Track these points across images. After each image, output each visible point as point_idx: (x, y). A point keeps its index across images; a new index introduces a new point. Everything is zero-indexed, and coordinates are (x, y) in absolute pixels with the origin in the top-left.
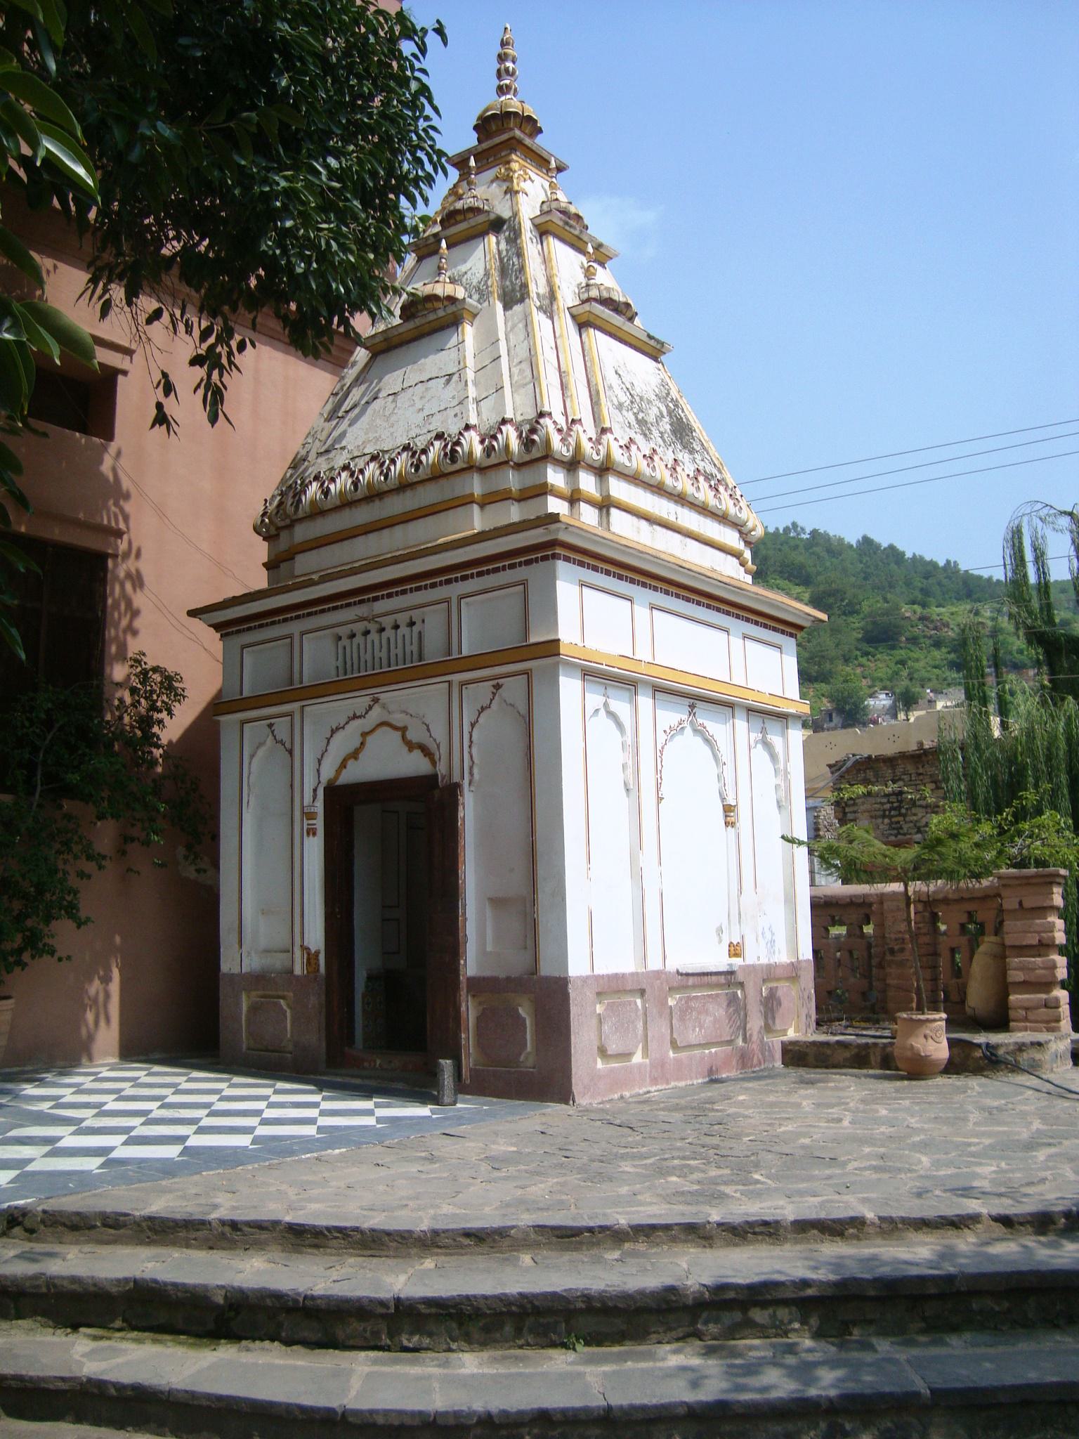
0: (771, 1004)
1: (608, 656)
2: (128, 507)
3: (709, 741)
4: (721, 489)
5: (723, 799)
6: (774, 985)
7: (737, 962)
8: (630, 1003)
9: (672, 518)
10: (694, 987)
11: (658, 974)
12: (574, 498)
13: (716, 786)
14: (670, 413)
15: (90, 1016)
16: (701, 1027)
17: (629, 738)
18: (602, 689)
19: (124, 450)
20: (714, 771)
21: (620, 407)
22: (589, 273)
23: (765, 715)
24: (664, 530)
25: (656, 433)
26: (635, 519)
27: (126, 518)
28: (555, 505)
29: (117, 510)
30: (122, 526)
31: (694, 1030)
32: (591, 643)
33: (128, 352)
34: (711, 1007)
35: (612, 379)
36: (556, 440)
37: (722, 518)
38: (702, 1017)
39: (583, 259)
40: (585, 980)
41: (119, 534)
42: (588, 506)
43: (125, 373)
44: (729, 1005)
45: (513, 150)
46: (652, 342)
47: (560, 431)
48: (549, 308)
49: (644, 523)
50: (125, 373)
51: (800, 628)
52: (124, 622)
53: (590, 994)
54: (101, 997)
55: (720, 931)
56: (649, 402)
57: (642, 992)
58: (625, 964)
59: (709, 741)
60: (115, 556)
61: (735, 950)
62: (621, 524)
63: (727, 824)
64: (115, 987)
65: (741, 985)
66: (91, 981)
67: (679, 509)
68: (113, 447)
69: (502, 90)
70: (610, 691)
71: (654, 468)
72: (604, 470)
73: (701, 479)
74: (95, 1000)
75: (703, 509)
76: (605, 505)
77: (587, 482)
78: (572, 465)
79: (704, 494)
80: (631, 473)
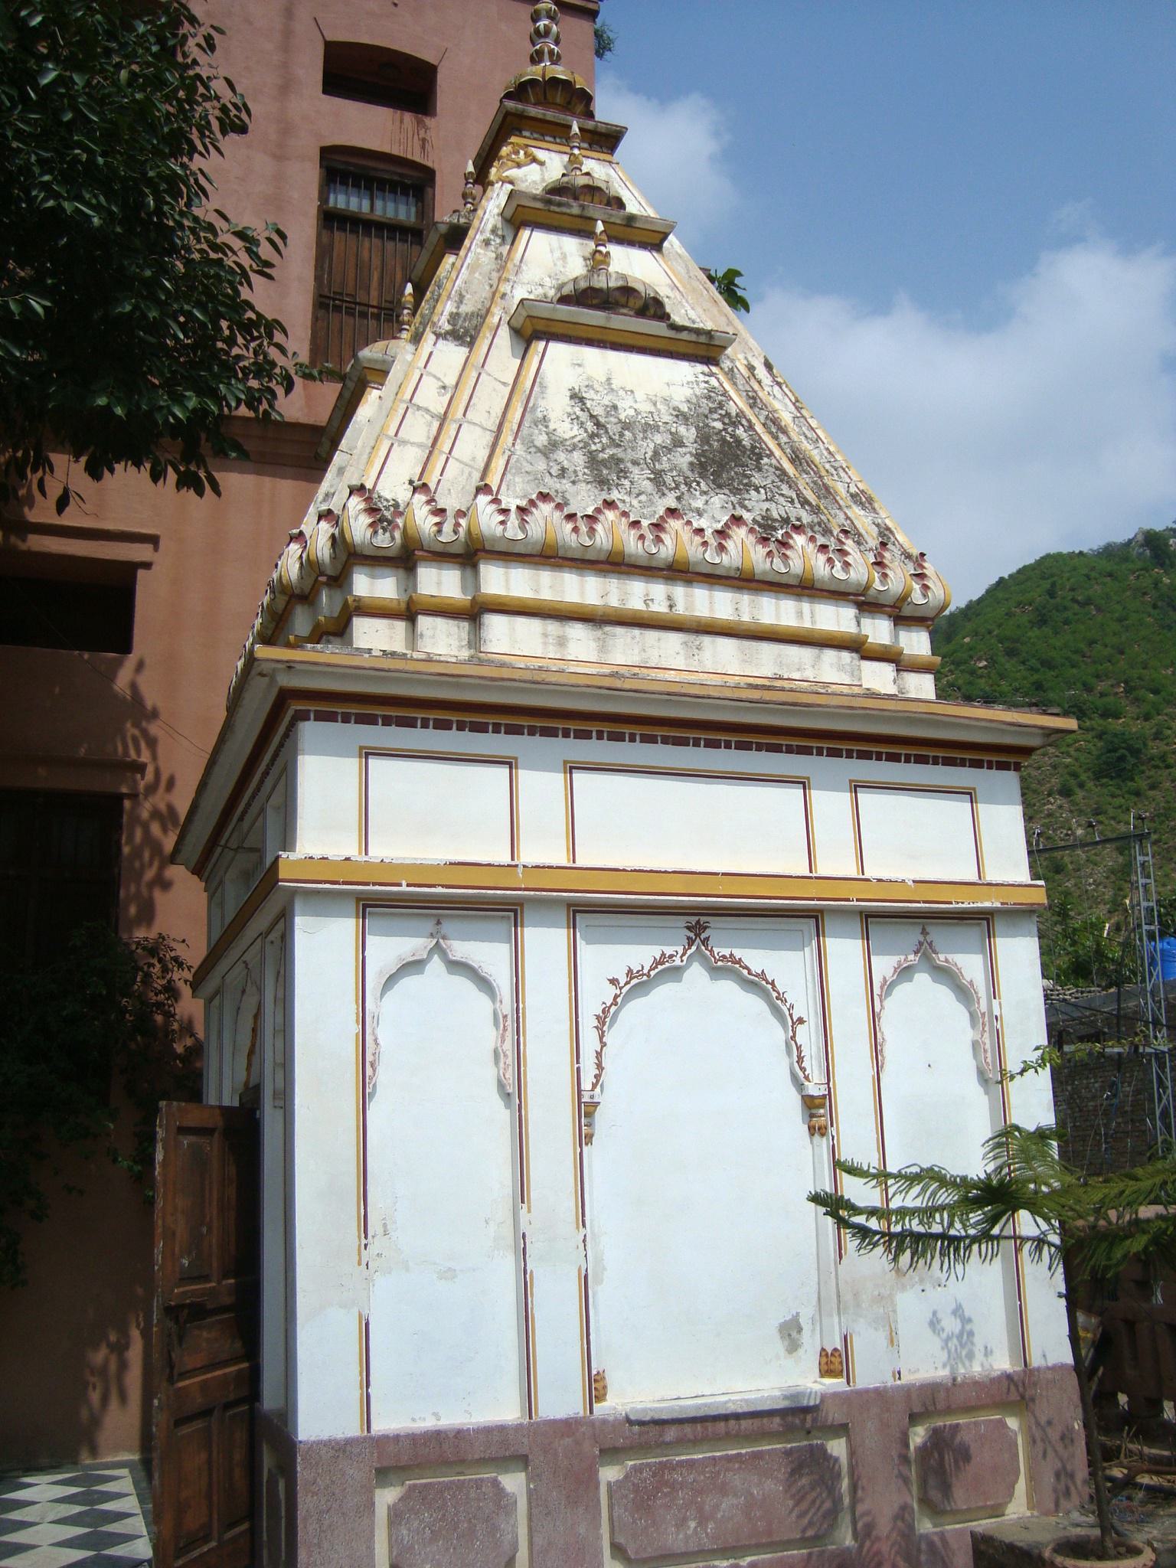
0: (940, 1466)
1: (435, 868)
2: (154, 729)
3: (758, 985)
4: (799, 540)
5: (799, 1086)
6: (940, 1423)
7: (834, 1384)
8: (479, 1484)
9: (660, 607)
10: (681, 1443)
11: (567, 1427)
12: (409, 612)
13: (781, 1067)
14: (704, 438)
15: (95, 1396)
16: (702, 1521)
17: (507, 1007)
18: (429, 925)
19: (147, 662)
20: (779, 1035)
21: (554, 445)
22: (597, 262)
23: (921, 923)
24: (636, 632)
25: (640, 477)
26: (553, 627)
27: (152, 743)
28: (374, 637)
29: (136, 732)
30: (145, 757)
31: (682, 1523)
32: (378, 851)
33: (153, 540)
34: (736, 1480)
35: (556, 406)
36: (359, 527)
37: (805, 588)
38: (709, 1501)
39: (591, 245)
40: (341, 1448)
41: (141, 768)
42: (440, 622)
43: (147, 565)
44: (796, 1472)
45: (518, 131)
46: (684, 335)
47: (372, 510)
48: (465, 333)
49: (577, 632)
50: (147, 565)
51: (1027, 751)
52: (150, 874)
53: (356, 1472)
54: (113, 1367)
55: (790, 1331)
56: (649, 428)
57: (521, 1461)
58: (502, 1409)
59: (758, 985)
60: (134, 796)
61: (834, 1363)
62: (506, 637)
63: (812, 1130)
64: (135, 1354)
65: (841, 1429)
66: (96, 1347)
67: (679, 591)
68: (131, 660)
69: (536, 58)
70: (447, 927)
71: (592, 531)
72: (470, 554)
73: (740, 533)
74: (103, 1371)
75: (744, 581)
76: (473, 613)
77: (440, 582)
78: (406, 558)
79: (744, 550)
80: (537, 549)
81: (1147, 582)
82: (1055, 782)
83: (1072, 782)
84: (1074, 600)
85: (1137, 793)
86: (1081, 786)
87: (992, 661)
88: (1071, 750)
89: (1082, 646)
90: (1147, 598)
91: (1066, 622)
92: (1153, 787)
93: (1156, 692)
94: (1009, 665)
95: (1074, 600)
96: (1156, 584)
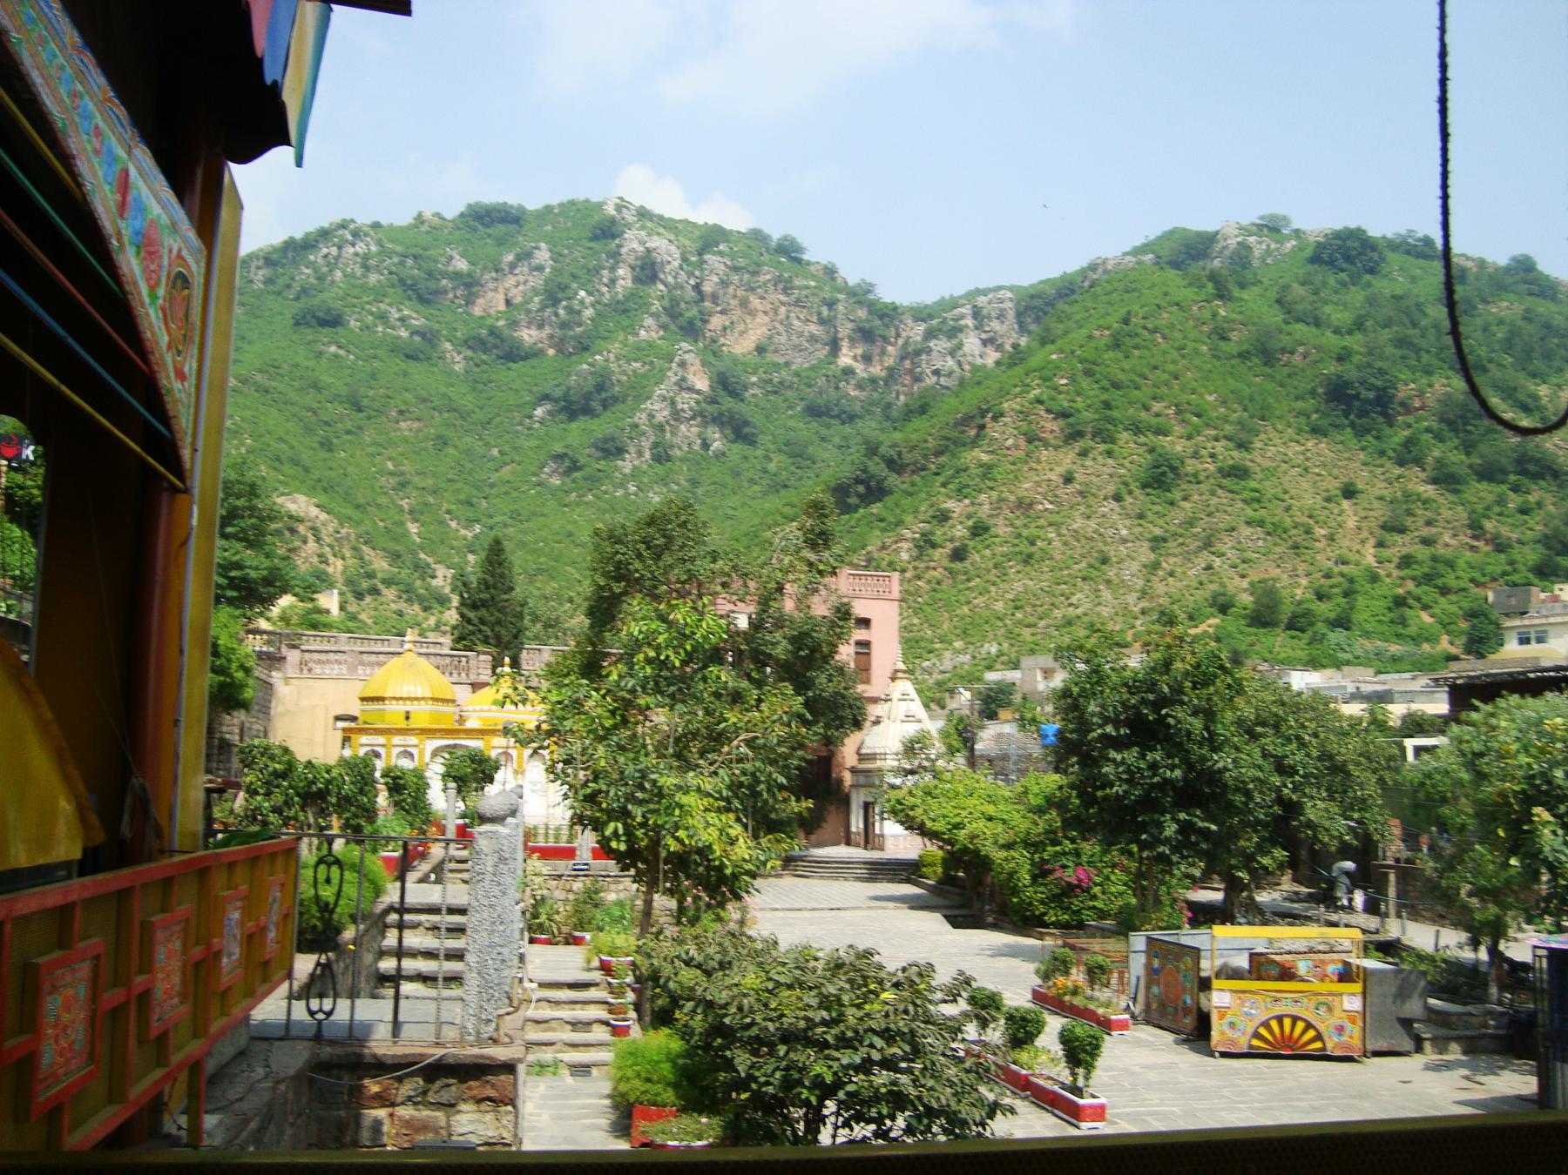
81: (1207, 315)
82: (1111, 489)
83: (1124, 490)
84: (1145, 328)
85: (1172, 504)
86: (1130, 493)
87: (1072, 379)
88: (1126, 462)
89: (1146, 371)
90: (1205, 328)
91: (1136, 347)
92: (1185, 499)
93: (1198, 416)
94: (1085, 383)
95: (1145, 328)
96: (1215, 315)
